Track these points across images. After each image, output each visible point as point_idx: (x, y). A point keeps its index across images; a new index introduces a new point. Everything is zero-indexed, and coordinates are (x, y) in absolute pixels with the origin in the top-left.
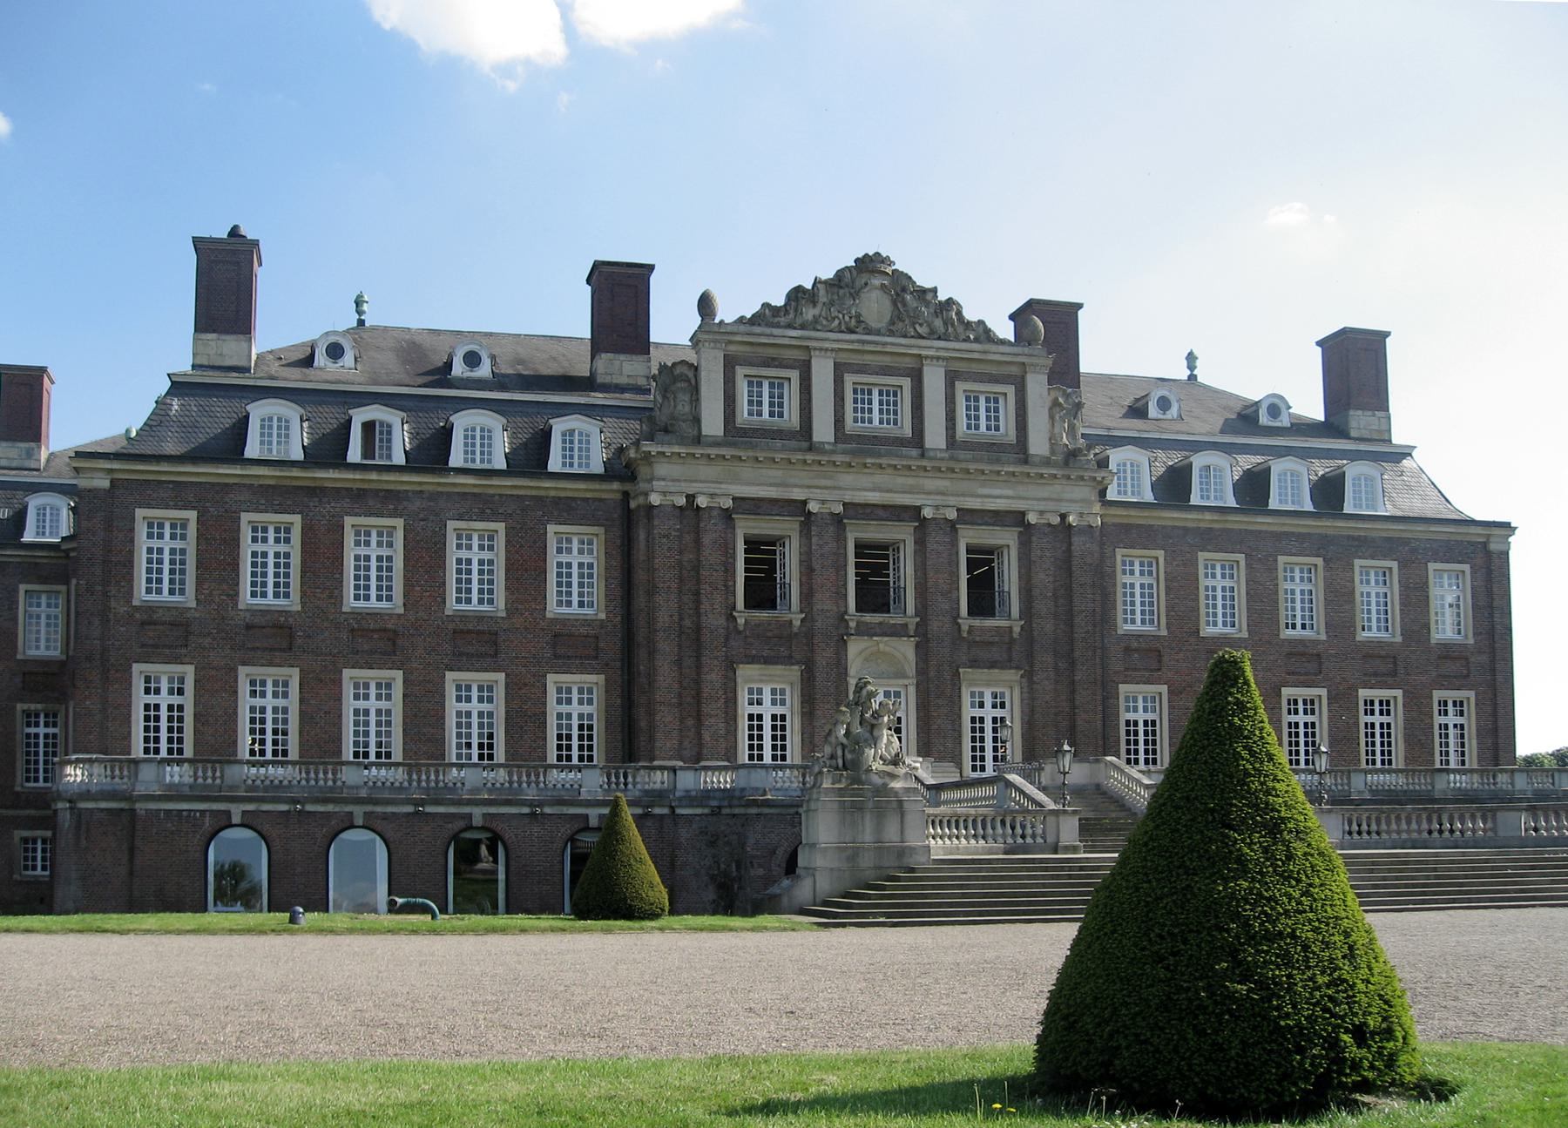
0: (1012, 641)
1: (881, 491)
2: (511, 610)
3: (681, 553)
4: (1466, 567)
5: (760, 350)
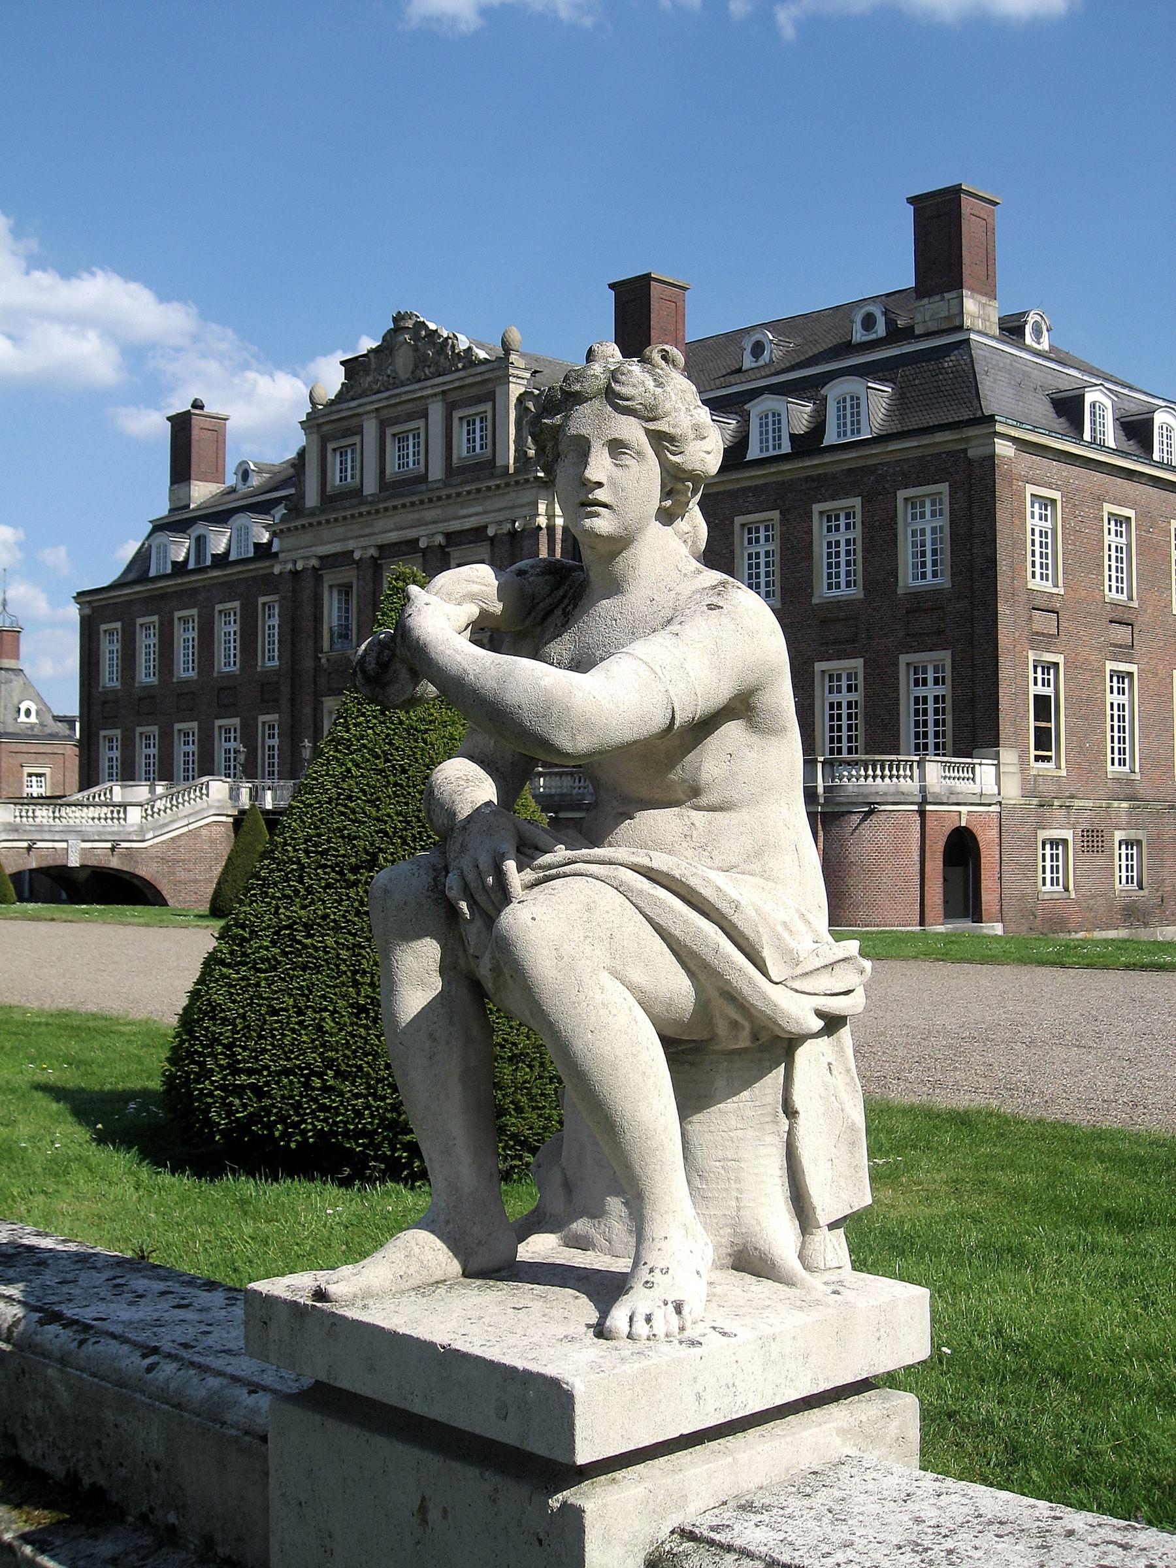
2: (242, 669)
4: (944, 487)
5: (338, 424)
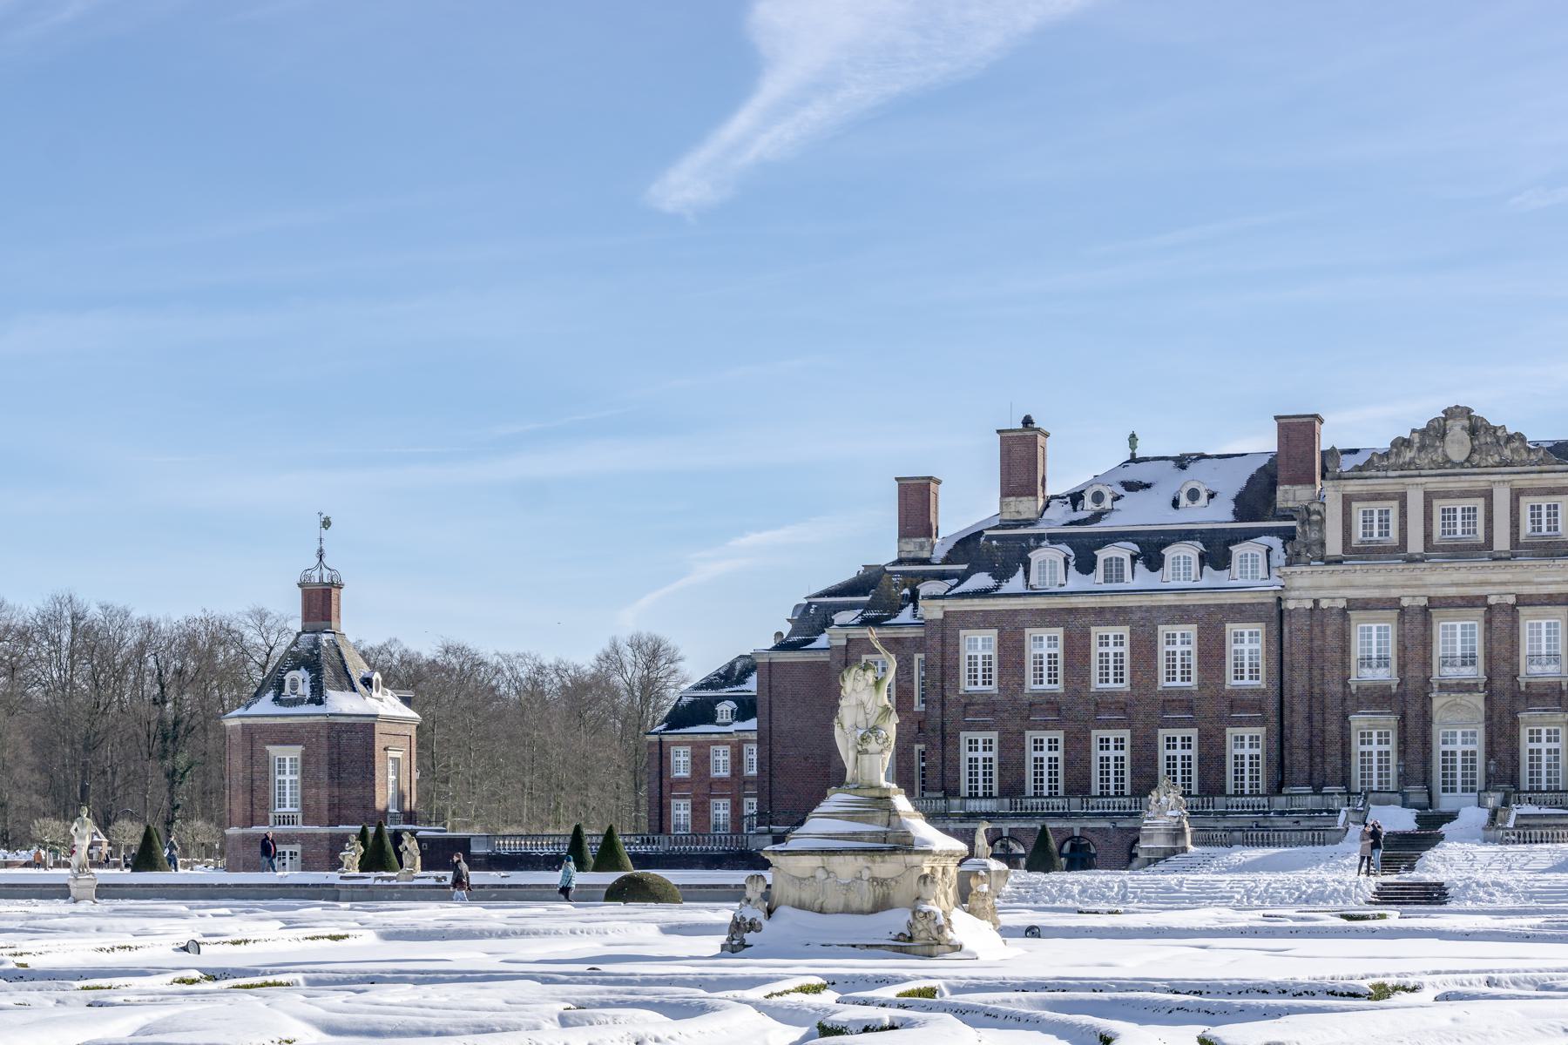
0: (1562, 692)
1: (1457, 585)
2: (1201, 685)
3: (1311, 640)
